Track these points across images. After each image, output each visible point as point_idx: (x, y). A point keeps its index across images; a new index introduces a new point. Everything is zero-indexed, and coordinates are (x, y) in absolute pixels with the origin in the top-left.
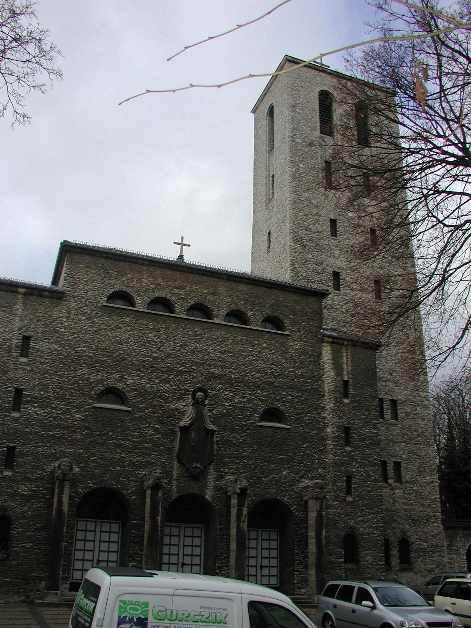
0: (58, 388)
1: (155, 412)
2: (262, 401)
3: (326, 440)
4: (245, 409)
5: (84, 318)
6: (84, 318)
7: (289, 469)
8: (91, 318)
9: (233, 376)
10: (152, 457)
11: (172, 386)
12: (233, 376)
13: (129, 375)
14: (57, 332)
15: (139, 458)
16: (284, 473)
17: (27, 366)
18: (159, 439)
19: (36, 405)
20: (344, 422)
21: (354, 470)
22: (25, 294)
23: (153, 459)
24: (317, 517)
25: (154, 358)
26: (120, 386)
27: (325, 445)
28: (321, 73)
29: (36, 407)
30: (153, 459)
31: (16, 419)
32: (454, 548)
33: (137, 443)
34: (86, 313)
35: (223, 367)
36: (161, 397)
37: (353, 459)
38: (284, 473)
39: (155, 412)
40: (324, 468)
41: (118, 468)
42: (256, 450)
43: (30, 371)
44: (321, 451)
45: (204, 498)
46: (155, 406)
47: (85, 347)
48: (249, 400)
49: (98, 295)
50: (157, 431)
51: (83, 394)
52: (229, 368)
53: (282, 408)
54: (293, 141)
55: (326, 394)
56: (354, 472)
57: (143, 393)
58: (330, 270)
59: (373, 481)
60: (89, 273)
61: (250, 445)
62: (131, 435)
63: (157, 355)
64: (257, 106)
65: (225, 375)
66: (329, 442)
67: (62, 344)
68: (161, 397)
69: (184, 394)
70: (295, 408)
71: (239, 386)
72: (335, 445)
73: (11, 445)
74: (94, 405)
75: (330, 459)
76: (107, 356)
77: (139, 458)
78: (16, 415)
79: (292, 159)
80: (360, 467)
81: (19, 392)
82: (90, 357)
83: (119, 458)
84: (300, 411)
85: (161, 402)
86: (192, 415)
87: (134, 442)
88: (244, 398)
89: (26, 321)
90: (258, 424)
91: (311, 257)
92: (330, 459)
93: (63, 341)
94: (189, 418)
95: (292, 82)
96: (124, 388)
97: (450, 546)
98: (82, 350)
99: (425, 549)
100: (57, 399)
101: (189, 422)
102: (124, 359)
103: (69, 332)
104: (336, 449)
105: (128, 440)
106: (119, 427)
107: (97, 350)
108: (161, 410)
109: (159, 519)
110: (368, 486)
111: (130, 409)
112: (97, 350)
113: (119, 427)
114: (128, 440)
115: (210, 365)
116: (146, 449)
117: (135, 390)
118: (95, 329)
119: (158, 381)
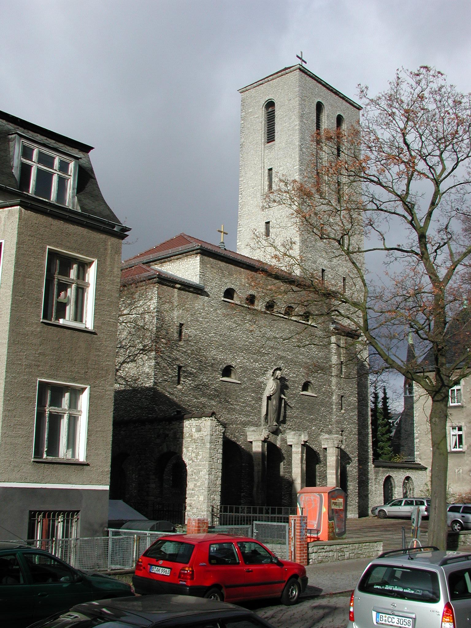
0: (201, 366)
1: (251, 384)
2: (303, 376)
3: (332, 405)
4: (294, 382)
5: (212, 310)
6: (212, 310)
7: (315, 425)
8: (216, 310)
9: (289, 357)
10: (251, 417)
11: (259, 364)
12: (289, 357)
13: (238, 355)
14: (198, 321)
15: (244, 418)
16: (313, 428)
17: (183, 348)
18: (254, 404)
19: (190, 379)
20: (341, 393)
21: (345, 426)
22: (179, 289)
23: (251, 419)
24: (336, 460)
25: (250, 343)
26: (233, 364)
27: (332, 409)
28: (318, 84)
29: (190, 380)
30: (251, 419)
31: (180, 390)
32: (378, 480)
33: (244, 407)
34: (213, 306)
35: (284, 350)
36: (254, 373)
37: (345, 419)
38: (313, 428)
39: (251, 384)
40: (331, 425)
41: (234, 426)
42: (300, 412)
43: (185, 352)
44: (330, 412)
45: (276, 446)
46: (252, 380)
47: (214, 333)
48: (297, 375)
49: (218, 291)
50: (253, 398)
51: (215, 371)
52: (287, 351)
53: (312, 382)
54: (301, 150)
55: (333, 371)
56: (345, 428)
57: (245, 369)
58: (320, 268)
59: (354, 435)
60: (212, 272)
61: (298, 409)
62: (240, 401)
63: (252, 341)
64: (247, 88)
65: (285, 357)
66: (334, 407)
67: (201, 331)
68: (254, 373)
69: (266, 371)
70: (318, 381)
71: (292, 365)
72: (337, 409)
73: (178, 410)
74: (221, 379)
75: (334, 418)
76: (225, 341)
77: (244, 418)
78: (179, 387)
79: (301, 168)
80: (348, 424)
81: (180, 367)
82: (217, 341)
83: (234, 418)
84: (321, 384)
85: (254, 377)
86: (273, 387)
87: (242, 406)
88: (294, 373)
89: (181, 311)
90: (301, 393)
91: (310, 256)
92: (334, 418)
93: (201, 328)
94: (272, 389)
95: (301, 91)
96: (236, 366)
97: (376, 479)
98: (212, 336)
99: (364, 480)
100: (201, 374)
101: (272, 392)
102: (234, 343)
103: (205, 321)
104: (337, 411)
105: (238, 405)
106: (234, 395)
107: (220, 335)
108: (254, 382)
109: (266, 462)
110: (351, 438)
111: (239, 382)
112: (220, 335)
113: (234, 395)
114: (238, 405)
115: (278, 349)
116: (248, 411)
117: (241, 367)
118: (218, 319)
119: (252, 361)
